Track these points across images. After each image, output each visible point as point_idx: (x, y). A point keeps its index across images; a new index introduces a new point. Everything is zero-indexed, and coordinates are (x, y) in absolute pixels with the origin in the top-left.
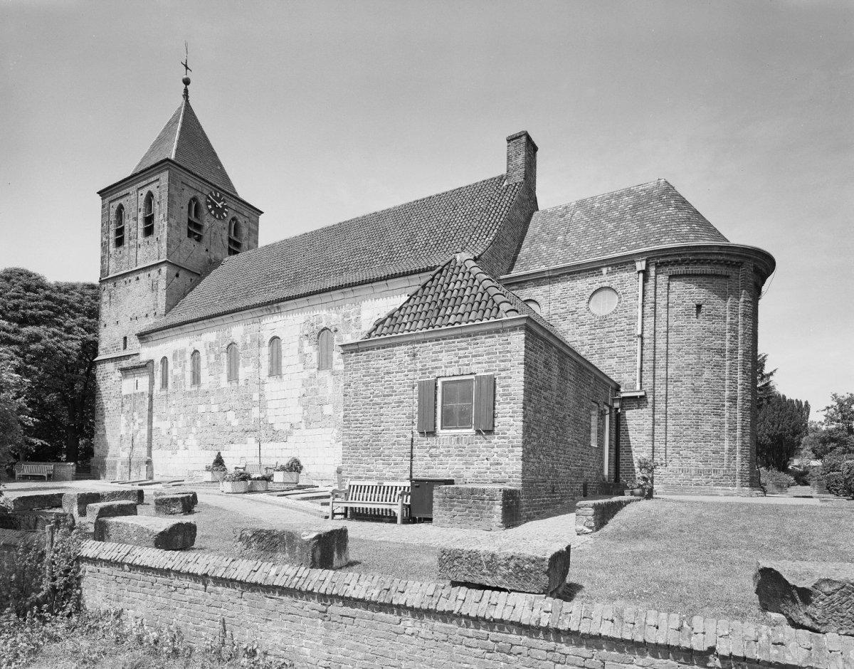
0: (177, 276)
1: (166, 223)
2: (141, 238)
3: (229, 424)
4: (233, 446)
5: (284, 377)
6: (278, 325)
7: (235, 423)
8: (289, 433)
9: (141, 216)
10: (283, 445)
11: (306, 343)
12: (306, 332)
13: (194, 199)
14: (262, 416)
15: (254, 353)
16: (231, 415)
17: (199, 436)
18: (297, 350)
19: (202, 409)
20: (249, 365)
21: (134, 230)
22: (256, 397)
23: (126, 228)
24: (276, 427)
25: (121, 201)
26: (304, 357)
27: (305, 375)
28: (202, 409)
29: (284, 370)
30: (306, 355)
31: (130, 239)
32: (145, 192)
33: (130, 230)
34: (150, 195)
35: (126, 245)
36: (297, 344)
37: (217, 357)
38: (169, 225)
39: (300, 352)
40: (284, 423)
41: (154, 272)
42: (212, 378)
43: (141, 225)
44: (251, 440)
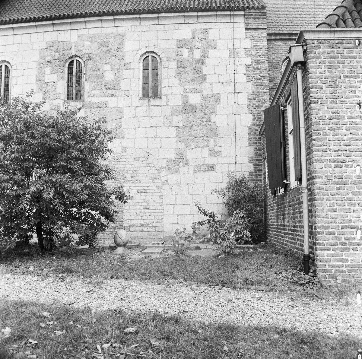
12: (48, 59)
18: (35, 77)
30: (47, 84)
36: (35, 72)
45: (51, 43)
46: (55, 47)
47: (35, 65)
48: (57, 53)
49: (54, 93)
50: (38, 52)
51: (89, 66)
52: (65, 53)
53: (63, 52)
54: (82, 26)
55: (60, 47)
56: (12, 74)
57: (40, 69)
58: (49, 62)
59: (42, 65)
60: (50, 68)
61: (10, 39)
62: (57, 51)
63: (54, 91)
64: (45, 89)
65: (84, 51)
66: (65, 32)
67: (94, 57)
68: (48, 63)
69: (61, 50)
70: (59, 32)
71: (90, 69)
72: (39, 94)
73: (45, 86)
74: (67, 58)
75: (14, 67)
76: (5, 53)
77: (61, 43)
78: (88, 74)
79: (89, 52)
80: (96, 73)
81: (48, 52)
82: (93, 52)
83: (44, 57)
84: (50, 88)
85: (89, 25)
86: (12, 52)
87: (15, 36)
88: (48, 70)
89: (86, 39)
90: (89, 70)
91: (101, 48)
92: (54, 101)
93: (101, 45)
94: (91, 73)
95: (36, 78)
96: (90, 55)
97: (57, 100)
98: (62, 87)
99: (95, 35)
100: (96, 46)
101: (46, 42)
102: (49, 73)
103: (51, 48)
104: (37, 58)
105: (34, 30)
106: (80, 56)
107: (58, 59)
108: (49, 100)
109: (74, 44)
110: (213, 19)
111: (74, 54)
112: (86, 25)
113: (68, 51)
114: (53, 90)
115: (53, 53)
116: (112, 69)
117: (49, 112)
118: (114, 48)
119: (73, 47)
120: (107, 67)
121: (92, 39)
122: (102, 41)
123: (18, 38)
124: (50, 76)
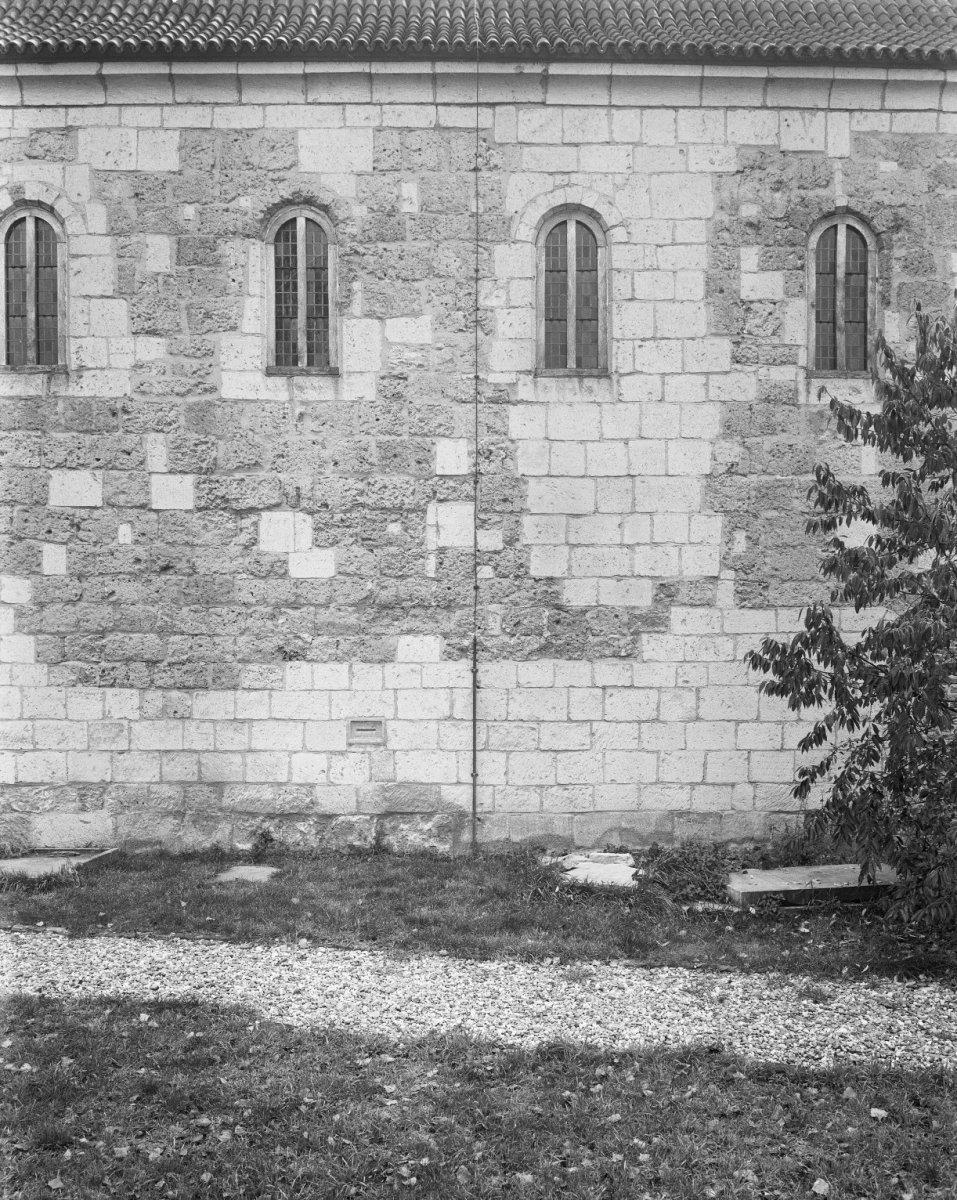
3: (277, 569)
4: (296, 673)
5: (630, 387)
6: (595, 160)
7: (314, 564)
8: (654, 621)
10: (608, 672)
12: (750, 211)
14: (491, 540)
15: (449, 259)
16: (283, 533)
17: (57, 617)
18: (701, 278)
19: (75, 489)
20: (415, 314)
22: (452, 457)
24: (576, 595)
26: (731, 312)
27: (745, 386)
28: (75, 489)
29: (620, 358)
30: (747, 306)
36: (701, 257)
37: (198, 254)
40: (619, 578)
42: (152, 349)
44: (420, 649)
45: (753, 154)
46: (771, 169)
47: (699, 233)
48: (778, 195)
49: (776, 341)
50: (707, 184)
51: (899, 252)
52: (811, 194)
53: (803, 192)
54: (871, 100)
55: (790, 172)
56: (616, 256)
57: (721, 248)
58: (750, 225)
59: (726, 235)
60: (756, 249)
61: (597, 125)
62: (779, 185)
63: (774, 334)
64: (741, 323)
65: (879, 196)
66: (807, 115)
67: (916, 220)
68: (749, 231)
69: (794, 184)
70: (785, 114)
71: (902, 263)
72: (717, 340)
73: (738, 312)
74: (815, 216)
75: (618, 234)
76: (580, 177)
77: (790, 158)
78: (895, 283)
79: (896, 200)
80: (924, 280)
81: (746, 190)
82: (911, 201)
83: (735, 207)
84: (758, 321)
85: (894, 101)
86: (606, 174)
87: (614, 111)
88: (750, 257)
89: (883, 150)
90: (897, 267)
91: (938, 191)
92: (773, 369)
94: (907, 279)
95: (707, 284)
96: (902, 211)
97: (783, 368)
98: (799, 326)
99: (913, 136)
101: (738, 149)
102: (756, 269)
103: (757, 174)
104: (706, 206)
105: (691, 97)
106: (865, 212)
107: (787, 217)
108: (753, 368)
109: (838, 165)
111: (842, 202)
112: (883, 99)
113: (821, 192)
114: (770, 331)
115: (767, 195)
117: (756, 408)
119: (838, 177)
122: (940, 162)
123: (626, 123)
124: (757, 282)
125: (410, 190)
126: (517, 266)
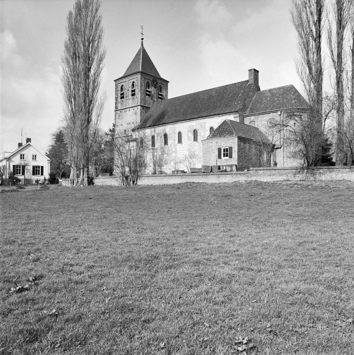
0: (143, 109)
1: (140, 92)
2: (130, 97)
9: (130, 89)
11: (189, 133)
13: (148, 82)
21: (128, 94)
23: (125, 93)
25: (123, 84)
27: (189, 143)
31: (126, 97)
32: (132, 81)
33: (126, 94)
34: (134, 82)
35: (125, 99)
38: (141, 93)
39: (188, 136)
41: (135, 108)
43: (130, 93)
93: (201, 126)
100: (200, 126)
110: (226, 116)
116: (203, 132)
118: (203, 126)
120: (202, 132)
121: (199, 124)
125: (171, 132)
126: (177, 136)
